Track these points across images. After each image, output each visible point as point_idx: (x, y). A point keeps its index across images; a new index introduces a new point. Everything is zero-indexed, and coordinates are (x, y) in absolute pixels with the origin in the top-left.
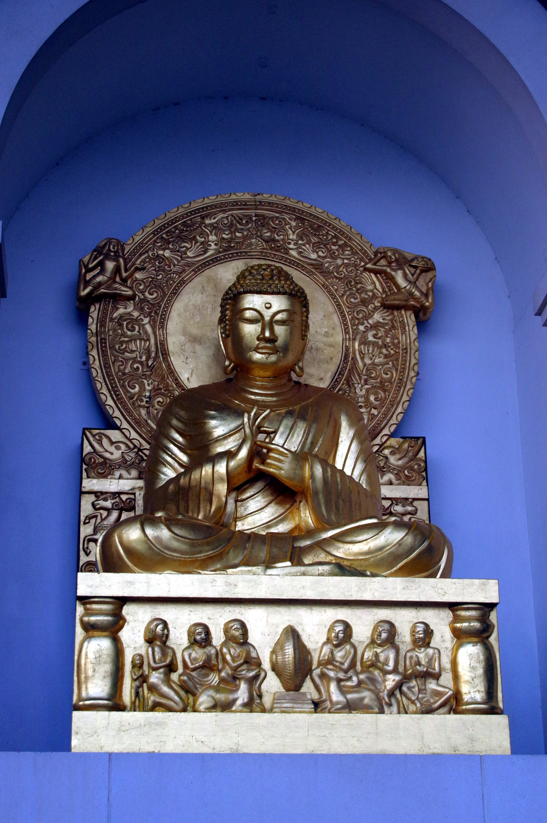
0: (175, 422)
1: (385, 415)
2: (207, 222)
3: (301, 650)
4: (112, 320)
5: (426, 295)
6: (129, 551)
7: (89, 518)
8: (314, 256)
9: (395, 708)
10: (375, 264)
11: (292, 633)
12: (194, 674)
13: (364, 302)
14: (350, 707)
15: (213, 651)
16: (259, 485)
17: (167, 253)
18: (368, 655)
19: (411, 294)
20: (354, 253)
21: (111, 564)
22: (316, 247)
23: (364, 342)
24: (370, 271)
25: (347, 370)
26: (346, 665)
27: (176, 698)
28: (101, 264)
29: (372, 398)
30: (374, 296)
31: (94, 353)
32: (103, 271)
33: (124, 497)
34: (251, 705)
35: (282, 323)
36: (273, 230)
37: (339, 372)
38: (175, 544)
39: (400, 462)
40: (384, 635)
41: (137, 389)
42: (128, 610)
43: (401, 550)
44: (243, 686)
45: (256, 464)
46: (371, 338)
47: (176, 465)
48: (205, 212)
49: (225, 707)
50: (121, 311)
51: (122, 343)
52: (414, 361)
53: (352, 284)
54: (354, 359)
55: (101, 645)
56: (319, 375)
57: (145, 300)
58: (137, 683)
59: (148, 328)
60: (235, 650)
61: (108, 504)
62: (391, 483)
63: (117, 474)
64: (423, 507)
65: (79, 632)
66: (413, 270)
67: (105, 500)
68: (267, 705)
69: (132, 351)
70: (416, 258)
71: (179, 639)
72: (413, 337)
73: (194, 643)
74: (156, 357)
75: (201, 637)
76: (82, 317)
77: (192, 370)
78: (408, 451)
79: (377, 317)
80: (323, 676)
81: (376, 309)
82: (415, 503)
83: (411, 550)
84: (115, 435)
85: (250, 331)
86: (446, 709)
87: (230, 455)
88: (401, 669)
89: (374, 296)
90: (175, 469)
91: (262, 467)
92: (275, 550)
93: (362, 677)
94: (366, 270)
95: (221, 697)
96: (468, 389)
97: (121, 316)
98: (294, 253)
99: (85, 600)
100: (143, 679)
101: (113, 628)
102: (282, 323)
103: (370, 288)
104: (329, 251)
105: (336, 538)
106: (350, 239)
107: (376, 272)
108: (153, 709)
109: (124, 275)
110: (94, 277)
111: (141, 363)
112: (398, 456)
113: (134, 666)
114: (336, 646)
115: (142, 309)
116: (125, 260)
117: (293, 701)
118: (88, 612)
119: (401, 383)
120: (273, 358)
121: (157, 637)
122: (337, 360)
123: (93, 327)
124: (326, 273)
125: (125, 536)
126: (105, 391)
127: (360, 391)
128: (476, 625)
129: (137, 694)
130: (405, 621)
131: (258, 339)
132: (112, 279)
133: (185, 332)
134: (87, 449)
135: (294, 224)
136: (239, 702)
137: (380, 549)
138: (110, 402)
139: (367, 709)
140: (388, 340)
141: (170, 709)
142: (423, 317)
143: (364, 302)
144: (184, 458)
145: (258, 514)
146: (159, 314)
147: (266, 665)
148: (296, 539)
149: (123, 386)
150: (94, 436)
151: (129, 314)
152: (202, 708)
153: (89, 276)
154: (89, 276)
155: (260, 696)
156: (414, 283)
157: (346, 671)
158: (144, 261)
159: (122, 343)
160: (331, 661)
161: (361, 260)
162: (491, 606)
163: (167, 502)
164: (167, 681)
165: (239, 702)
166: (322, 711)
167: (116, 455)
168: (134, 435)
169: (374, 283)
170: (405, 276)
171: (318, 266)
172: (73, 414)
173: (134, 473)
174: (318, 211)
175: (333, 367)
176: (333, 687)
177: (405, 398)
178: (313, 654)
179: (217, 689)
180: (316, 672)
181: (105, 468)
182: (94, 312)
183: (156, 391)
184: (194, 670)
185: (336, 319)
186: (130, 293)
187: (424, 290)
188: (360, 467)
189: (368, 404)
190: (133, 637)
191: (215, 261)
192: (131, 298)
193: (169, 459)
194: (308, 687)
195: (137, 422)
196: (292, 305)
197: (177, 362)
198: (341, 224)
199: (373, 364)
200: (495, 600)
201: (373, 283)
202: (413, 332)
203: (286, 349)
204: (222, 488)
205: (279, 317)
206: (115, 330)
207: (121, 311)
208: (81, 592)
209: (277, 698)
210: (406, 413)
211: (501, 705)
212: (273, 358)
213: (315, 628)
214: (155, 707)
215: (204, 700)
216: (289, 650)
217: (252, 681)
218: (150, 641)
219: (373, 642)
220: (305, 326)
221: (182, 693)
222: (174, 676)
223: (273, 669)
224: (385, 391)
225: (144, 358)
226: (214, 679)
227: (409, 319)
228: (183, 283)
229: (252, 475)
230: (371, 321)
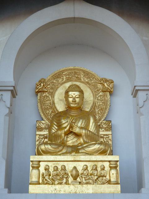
0: (55, 120)
1: (102, 116)
2: (63, 74)
3: (77, 171)
4: (43, 96)
5: (112, 88)
6: (43, 151)
7: (38, 140)
8: (87, 80)
9: (96, 183)
11: (75, 168)
12: (54, 176)
13: (98, 90)
14: (87, 183)
15: (58, 172)
16: (72, 134)
17: (55, 81)
18: (91, 172)
19: (108, 89)
20: (96, 79)
21: (39, 154)
22: (87, 78)
23: (98, 99)
24: (99, 83)
25: (94, 106)
26: (86, 175)
28: (40, 84)
29: (99, 112)
30: (100, 89)
31: (39, 104)
32: (40, 86)
33: (45, 136)
34: (66, 183)
35: (77, 98)
36: (78, 75)
37: (92, 106)
38: (52, 149)
39: (106, 126)
40: (94, 168)
41: (48, 112)
42: (41, 163)
43: (99, 149)
45: (71, 130)
46: (99, 99)
47: (55, 129)
48: (63, 71)
49: (61, 184)
50: (45, 94)
51: (45, 101)
52: (109, 103)
53: (95, 86)
54: (96, 103)
55: (35, 172)
56: (87, 109)
57: (50, 92)
58: (43, 179)
59: (51, 98)
60: (63, 172)
61: (42, 137)
62: (103, 131)
63: (44, 130)
64: (110, 136)
66: (109, 83)
67: (41, 136)
68: (70, 183)
69: (47, 103)
70: (110, 80)
71: (51, 170)
72: (109, 98)
73: (54, 170)
74: (52, 104)
75: (56, 169)
76: (37, 95)
77: (61, 107)
78: (107, 124)
80: (81, 177)
81: (100, 92)
82: (109, 135)
83: (101, 149)
84: (43, 122)
85: (71, 100)
86: (106, 184)
87: (65, 128)
88: (98, 175)
89: (100, 89)
90: (54, 130)
91: (72, 130)
92: (73, 149)
93: (90, 177)
94: (98, 83)
95: (60, 181)
96: (122, 109)
97: (45, 95)
99: (31, 161)
100: (44, 178)
101: (38, 168)
102: (77, 98)
104: (90, 79)
105: (86, 147)
106: (95, 76)
107: (100, 84)
108: (46, 184)
109: (45, 86)
110: (39, 87)
112: (105, 125)
113: (42, 175)
114: (84, 170)
117: (75, 182)
119: (106, 108)
120: (76, 105)
121: (47, 169)
122: (92, 104)
123: (39, 98)
124: (90, 84)
125: (41, 147)
126: (41, 112)
127: (97, 111)
128: (114, 165)
129: (43, 181)
130: (99, 164)
131: (72, 101)
132: (43, 87)
133: (58, 99)
134: (37, 125)
135: (82, 73)
136: (64, 182)
138: (42, 115)
139: (90, 184)
140: (103, 99)
141: (50, 184)
142: (111, 93)
143: (98, 90)
144: (57, 128)
145: (71, 141)
146: (53, 95)
147: (70, 175)
148: (78, 146)
149: (45, 111)
150: (39, 122)
151: (46, 95)
152: (56, 184)
153: (38, 87)
154: (38, 87)
155: (68, 181)
156: (109, 86)
157: (86, 176)
158: (50, 83)
159: (45, 101)
160: (82, 174)
161: (97, 81)
162: (117, 161)
163: (52, 138)
164: (49, 178)
165: (64, 182)
167: (44, 126)
168: (47, 122)
169: (100, 86)
170: (107, 84)
171: (88, 83)
172: (34, 118)
173: (47, 130)
174: (88, 70)
175: (91, 105)
176: (84, 179)
177: (107, 112)
178: (79, 172)
180: (80, 176)
181: (40, 129)
182: (39, 94)
183: (52, 112)
184: (55, 176)
185: (92, 94)
186: (47, 90)
187: (111, 87)
188: (94, 129)
189: (98, 113)
190: (42, 169)
191: (65, 82)
192: (46, 92)
193: (53, 128)
194: (78, 179)
195: (48, 119)
197: (57, 105)
198: (93, 73)
199: (100, 104)
200: (118, 160)
201: (100, 86)
202: (109, 97)
203: (78, 104)
204: (63, 135)
205: (76, 97)
206: (43, 99)
207: (45, 94)
208: (31, 160)
209: (72, 182)
210: (107, 115)
211: (119, 182)
213: (80, 167)
214: (46, 184)
215: (56, 182)
216: (74, 172)
217: (66, 178)
218: (46, 170)
219: (92, 169)
220: (83, 97)
221: (52, 181)
222: (50, 177)
223: (71, 175)
224: (102, 110)
225: (49, 105)
226: (58, 178)
227: (108, 94)
228: (58, 88)
229: (70, 132)
230: (99, 95)
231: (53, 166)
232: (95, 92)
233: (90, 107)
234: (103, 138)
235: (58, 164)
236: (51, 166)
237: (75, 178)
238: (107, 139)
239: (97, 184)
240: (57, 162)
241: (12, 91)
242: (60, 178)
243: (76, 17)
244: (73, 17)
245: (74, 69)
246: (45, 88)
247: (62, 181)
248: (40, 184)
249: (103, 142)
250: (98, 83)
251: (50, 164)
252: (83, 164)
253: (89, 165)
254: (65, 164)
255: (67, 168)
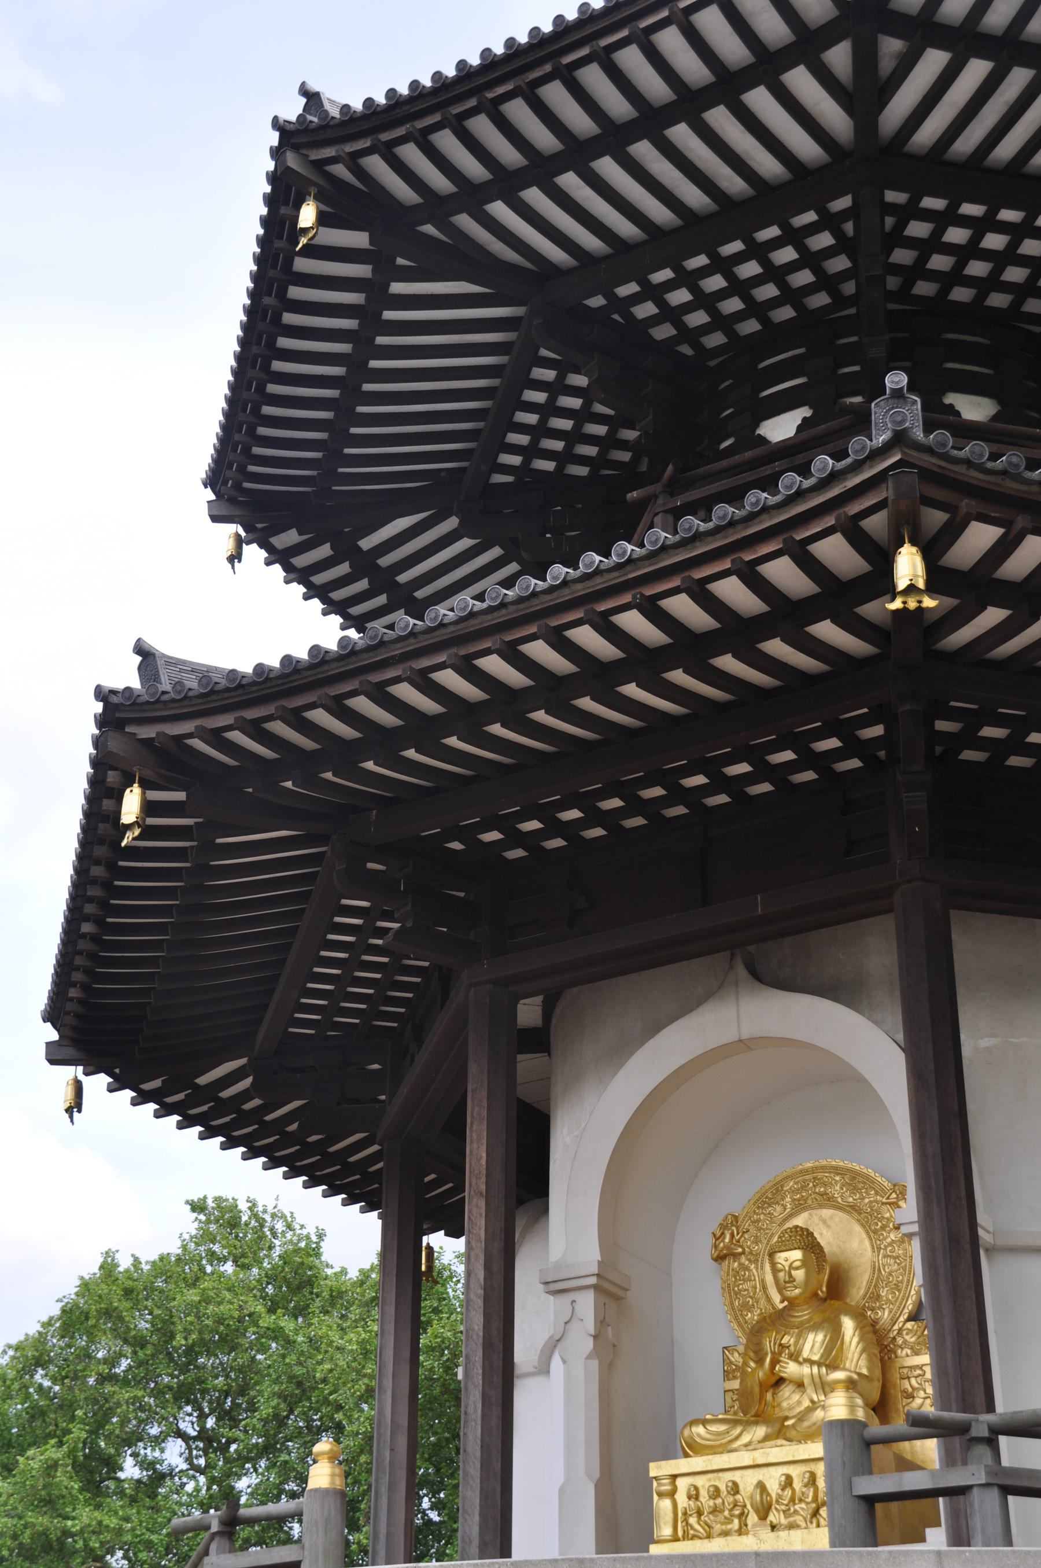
8: (851, 1199)
9: (814, 1524)
10: (888, 1198)
11: (761, 1486)
13: (883, 1228)
14: (791, 1526)
20: (877, 1193)
27: (702, 1530)
32: (723, 1241)
34: (740, 1532)
35: (797, 1268)
36: (825, 1185)
38: (708, 1436)
39: (913, 1339)
44: (736, 1521)
54: (879, 1270)
55: (667, 1503)
59: (754, 1271)
60: (731, 1499)
65: (655, 1497)
75: (716, 1493)
79: (892, 1236)
81: (891, 1230)
98: (839, 1200)
100: (686, 1520)
101: (672, 1494)
103: (888, 1215)
106: (873, 1182)
107: (890, 1204)
108: (692, 1539)
111: (751, 1298)
115: (749, 1260)
116: (738, 1228)
118: (659, 1485)
120: (797, 1291)
121: (694, 1495)
127: (883, 1293)
135: (837, 1178)
137: (815, 1424)
139: (798, 1526)
141: (700, 1538)
155: (746, 1525)
166: (778, 1530)
179: (722, 1524)
185: (867, 1243)
186: (740, 1250)
189: (888, 1301)
190: (681, 1498)
192: (743, 1253)
194: (772, 1518)
196: (804, 1255)
208: (652, 1474)
209: (754, 1525)
212: (797, 1291)
213: (773, 1479)
214: (693, 1537)
215: (718, 1528)
218: (689, 1498)
224: (899, 1291)
226: (721, 1518)
231: (708, 1484)
232: (875, 1232)
233: (864, 1283)
234: (909, 1378)
235: (719, 1479)
236: (703, 1486)
237: (763, 1517)
238: (919, 1379)
239: (818, 1526)
240: (715, 1474)
241: (596, 1287)
242: (726, 1518)
243: (743, 1037)
244: (737, 1039)
245: (814, 1170)
246: (738, 1241)
247: (729, 1527)
248: (678, 1540)
249: (910, 1390)
250: (883, 1203)
251: (701, 1482)
252: (778, 1472)
253: (795, 1471)
254: (736, 1476)
255: (741, 1488)
